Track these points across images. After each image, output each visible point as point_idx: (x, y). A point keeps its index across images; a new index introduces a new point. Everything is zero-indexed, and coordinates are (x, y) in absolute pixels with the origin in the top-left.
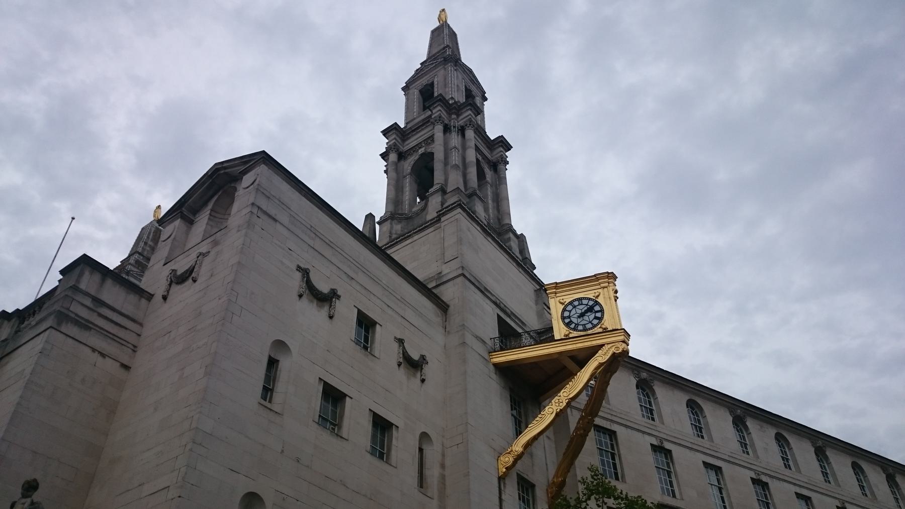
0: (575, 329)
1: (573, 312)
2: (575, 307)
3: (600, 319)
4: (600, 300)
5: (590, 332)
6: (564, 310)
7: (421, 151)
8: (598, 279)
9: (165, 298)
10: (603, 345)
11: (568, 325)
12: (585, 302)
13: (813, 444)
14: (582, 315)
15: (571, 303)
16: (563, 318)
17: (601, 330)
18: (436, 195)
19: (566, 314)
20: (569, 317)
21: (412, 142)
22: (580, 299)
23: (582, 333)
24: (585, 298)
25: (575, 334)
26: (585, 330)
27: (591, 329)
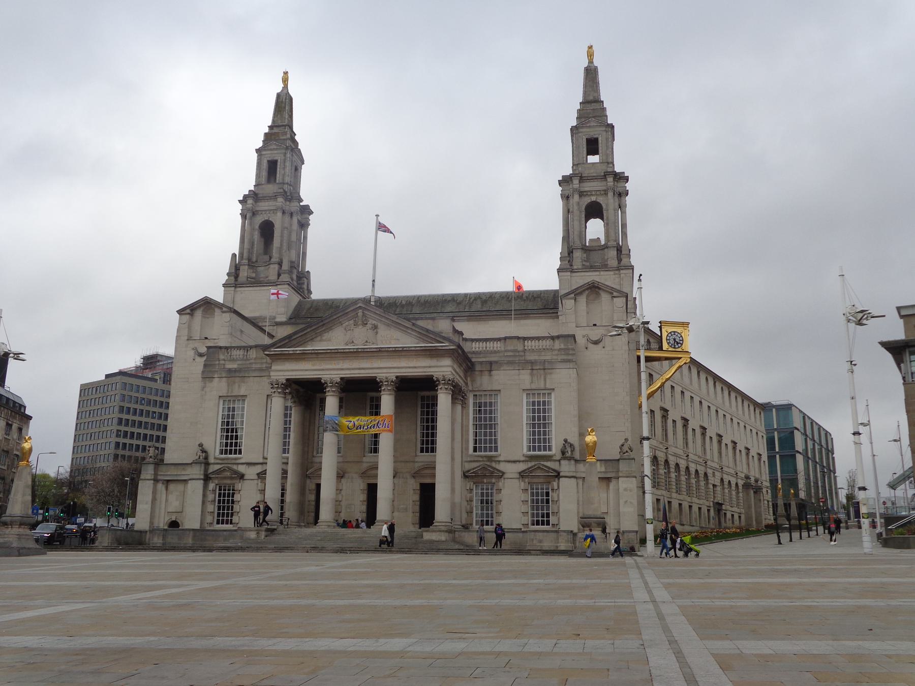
0: (671, 346)
1: (671, 338)
2: (672, 335)
3: (682, 344)
4: (683, 335)
5: (677, 350)
6: (667, 336)
7: (593, 198)
8: (683, 324)
9: (587, 348)
10: (681, 358)
11: (668, 343)
12: (676, 334)
13: (697, 369)
14: (674, 339)
15: (670, 333)
16: (667, 340)
17: (681, 350)
18: (612, 249)
19: (668, 338)
20: (669, 340)
21: (588, 186)
22: (674, 332)
23: (674, 350)
24: (677, 332)
25: (670, 349)
26: (674, 348)
27: (678, 348)
